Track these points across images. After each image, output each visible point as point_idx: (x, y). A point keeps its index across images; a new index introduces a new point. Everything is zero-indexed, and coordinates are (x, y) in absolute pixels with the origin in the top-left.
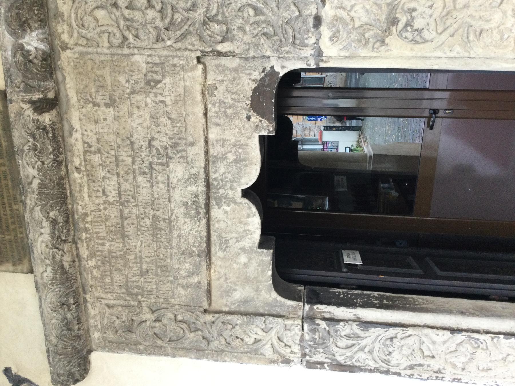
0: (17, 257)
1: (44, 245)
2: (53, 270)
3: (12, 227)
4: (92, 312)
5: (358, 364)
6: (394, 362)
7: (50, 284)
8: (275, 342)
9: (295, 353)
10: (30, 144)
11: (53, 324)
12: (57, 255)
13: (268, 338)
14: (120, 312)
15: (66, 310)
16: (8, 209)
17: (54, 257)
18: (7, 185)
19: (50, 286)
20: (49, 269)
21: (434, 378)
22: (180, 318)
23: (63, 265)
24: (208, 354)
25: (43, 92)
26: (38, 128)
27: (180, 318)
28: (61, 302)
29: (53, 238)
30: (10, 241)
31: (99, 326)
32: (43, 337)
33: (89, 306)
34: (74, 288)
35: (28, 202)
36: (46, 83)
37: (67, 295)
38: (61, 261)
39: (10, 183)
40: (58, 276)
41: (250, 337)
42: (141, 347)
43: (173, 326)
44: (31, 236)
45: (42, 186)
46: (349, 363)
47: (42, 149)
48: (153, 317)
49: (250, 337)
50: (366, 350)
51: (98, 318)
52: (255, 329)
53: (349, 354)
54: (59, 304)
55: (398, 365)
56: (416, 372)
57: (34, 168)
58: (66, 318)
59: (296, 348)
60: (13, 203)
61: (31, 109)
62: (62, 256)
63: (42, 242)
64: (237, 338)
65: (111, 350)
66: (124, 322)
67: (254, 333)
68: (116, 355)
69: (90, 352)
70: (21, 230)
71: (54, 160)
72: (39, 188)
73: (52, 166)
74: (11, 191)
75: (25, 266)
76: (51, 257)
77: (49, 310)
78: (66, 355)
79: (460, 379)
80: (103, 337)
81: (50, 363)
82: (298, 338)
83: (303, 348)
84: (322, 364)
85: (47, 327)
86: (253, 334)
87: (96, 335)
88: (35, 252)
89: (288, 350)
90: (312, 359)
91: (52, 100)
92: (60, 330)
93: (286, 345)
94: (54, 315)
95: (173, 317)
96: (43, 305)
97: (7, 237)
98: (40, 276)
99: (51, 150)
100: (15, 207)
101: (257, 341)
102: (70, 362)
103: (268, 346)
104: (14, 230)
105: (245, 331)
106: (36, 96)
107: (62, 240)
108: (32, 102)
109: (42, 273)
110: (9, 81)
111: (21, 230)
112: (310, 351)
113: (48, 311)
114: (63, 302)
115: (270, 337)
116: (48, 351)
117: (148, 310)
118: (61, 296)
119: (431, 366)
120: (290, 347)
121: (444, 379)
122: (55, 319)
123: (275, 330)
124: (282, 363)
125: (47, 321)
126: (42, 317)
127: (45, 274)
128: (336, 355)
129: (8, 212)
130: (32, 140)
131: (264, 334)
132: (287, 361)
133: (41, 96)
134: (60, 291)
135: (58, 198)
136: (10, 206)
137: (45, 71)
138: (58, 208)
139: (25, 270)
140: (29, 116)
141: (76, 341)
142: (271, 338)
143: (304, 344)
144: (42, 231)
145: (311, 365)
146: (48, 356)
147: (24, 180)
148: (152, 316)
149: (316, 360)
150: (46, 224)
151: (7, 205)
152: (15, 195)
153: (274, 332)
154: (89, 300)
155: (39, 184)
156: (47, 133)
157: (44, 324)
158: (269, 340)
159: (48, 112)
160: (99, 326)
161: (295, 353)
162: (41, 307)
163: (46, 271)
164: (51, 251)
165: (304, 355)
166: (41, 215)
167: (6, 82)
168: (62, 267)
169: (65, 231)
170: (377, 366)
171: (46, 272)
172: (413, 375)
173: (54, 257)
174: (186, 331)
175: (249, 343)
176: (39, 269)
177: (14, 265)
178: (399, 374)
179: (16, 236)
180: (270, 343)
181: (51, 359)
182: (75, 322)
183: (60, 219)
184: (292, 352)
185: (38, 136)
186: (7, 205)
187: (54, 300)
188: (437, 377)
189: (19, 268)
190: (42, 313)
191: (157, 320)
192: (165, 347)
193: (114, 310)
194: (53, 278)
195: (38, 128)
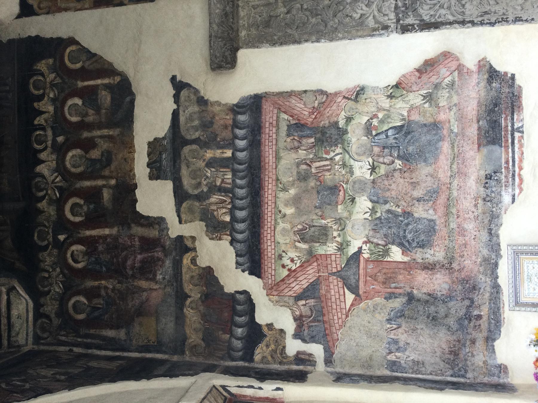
4: (242, 14)
5: (439, 20)
6: (467, 12)
8: (376, 13)
9: (391, 20)
13: (371, 11)
14: (262, 10)
21: (500, 20)
22: (305, 7)
24: (326, 33)
27: (305, 7)
31: (246, 25)
33: (240, 9)
41: (357, 13)
42: (276, 38)
43: (300, 14)
46: (433, 20)
48: (285, 10)
49: (357, 13)
50: (445, 6)
51: (246, 19)
52: (361, 5)
53: (432, 13)
55: (471, 15)
56: (486, 17)
59: (392, 16)
64: (347, 16)
65: (254, 46)
66: (264, 18)
67: (360, 8)
68: (256, 50)
69: (237, 49)
78: (223, 38)
79: (521, 17)
80: (248, 34)
82: (393, 6)
83: (397, 15)
84: (413, 25)
85: (212, 16)
86: (359, 9)
87: (243, 33)
89: (386, 18)
90: (405, 22)
93: (384, 15)
95: (300, 6)
101: (362, 15)
102: (225, 45)
103: (371, 17)
105: (353, 9)
112: (403, 16)
113: (214, 3)
115: (372, 10)
116: (210, 36)
117: (282, 5)
119: (497, 11)
120: (387, 15)
121: (508, 20)
123: (376, 3)
124: (382, 29)
125: (212, 11)
128: (423, 15)
131: (368, 9)
132: (386, 28)
142: (373, 11)
143: (398, 11)
145: (405, 29)
146: (210, 41)
148: (285, 9)
149: (407, 23)
153: (375, 5)
154: (240, 4)
157: (210, 14)
158: (371, 13)
160: (246, 25)
161: (391, 20)
165: (398, 21)
170: (455, 19)
172: (483, 20)
174: (310, 18)
175: (356, 18)
178: (473, 23)
180: (372, 15)
181: (212, 43)
184: (389, 19)
188: (502, 18)
191: (288, 13)
192: (293, 35)
193: (258, 10)
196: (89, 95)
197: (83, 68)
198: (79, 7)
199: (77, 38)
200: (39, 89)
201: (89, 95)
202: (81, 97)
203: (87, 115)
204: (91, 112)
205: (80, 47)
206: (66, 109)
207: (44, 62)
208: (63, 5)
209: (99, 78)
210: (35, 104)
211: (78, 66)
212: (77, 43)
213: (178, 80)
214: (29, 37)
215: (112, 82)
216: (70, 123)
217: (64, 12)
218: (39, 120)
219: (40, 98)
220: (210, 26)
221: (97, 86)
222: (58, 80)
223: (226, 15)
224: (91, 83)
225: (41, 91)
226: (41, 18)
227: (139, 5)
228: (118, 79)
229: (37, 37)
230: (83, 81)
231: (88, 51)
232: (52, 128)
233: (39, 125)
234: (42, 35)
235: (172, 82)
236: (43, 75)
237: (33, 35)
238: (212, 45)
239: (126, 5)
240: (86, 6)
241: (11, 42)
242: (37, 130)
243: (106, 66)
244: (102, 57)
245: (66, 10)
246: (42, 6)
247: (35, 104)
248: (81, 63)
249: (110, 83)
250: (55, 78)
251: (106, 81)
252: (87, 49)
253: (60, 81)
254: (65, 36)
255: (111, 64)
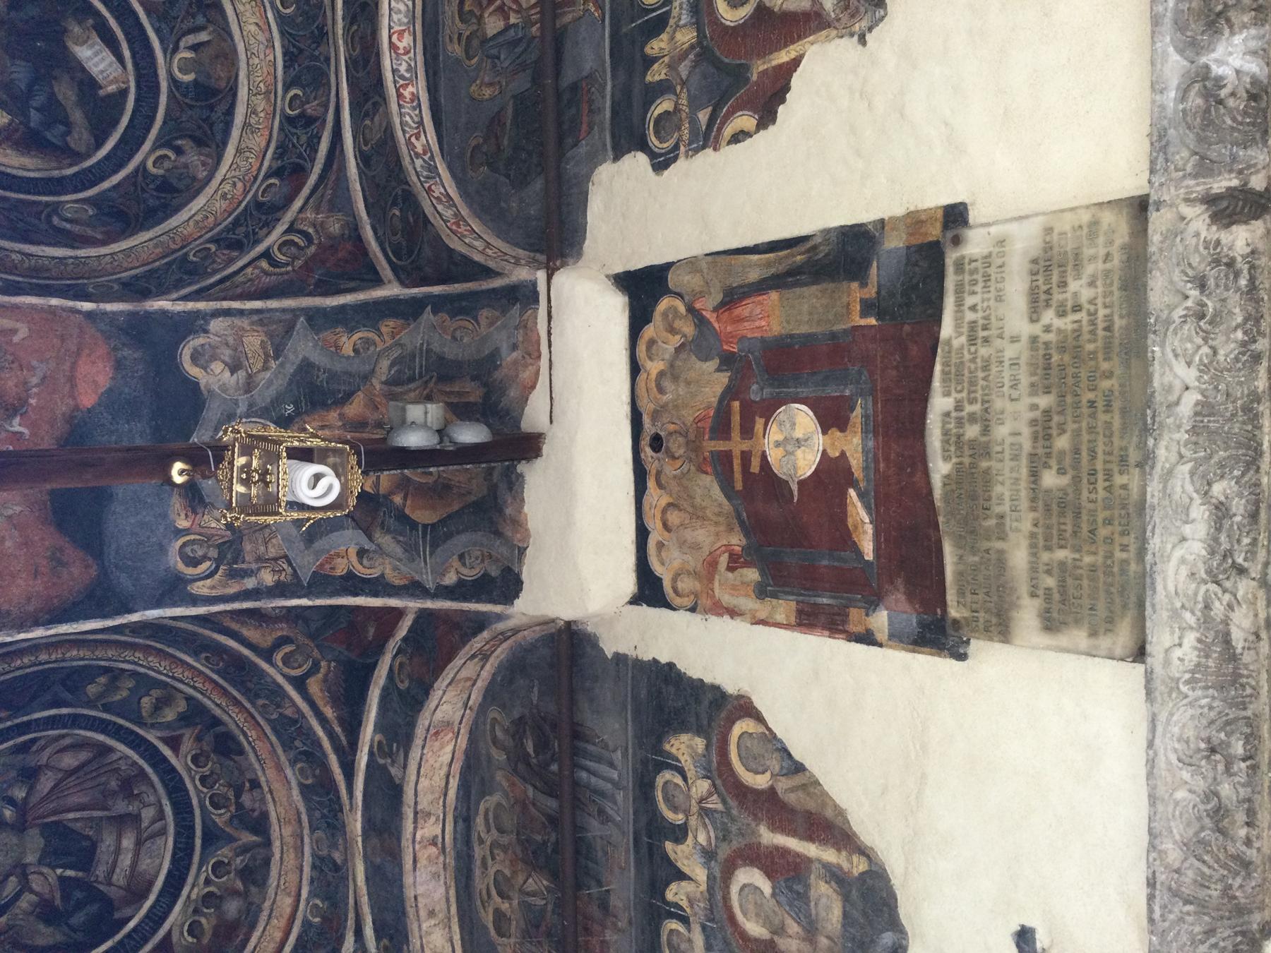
0: (1102, 611)
1: (1184, 571)
2: (1199, 641)
3: (1103, 532)
7: (1187, 682)
10: (1189, 303)
11: (1177, 803)
12: (1217, 604)
15: (1221, 767)
16: (1101, 484)
17: (1207, 607)
18: (1108, 425)
19: (1184, 689)
20: (1190, 639)
23: (1227, 634)
25: (1240, 172)
26: (1216, 262)
28: (1208, 740)
29: (1212, 553)
30: (1093, 568)
32: (1146, 838)
34: (1249, 713)
35: (1161, 453)
36: (1249, 152)
37: (1228, 723)
38: (1226, 622)
39: (1117, 423)
40: (1211, 663)
44: (1155, 543)
45: (1205, 409)
47: (1217, 314)
54: (1203, 746)
57: (1189, 364)
58: (1216, 794)
60: (1116, 469)
61: (1206, 216)
62: (1230, 607)
63: (1183, 561)
70: (1125, 540)
71: (1244, 344)
72: (1196, 414)
73: (1237, 359)
74: (1116, 440)
75: (1123, 638)
76: (1200, 606)
77: (1173, 758)
78: (1202, 906)
81: (1151, 920)
85: (1160, 808)
88: (1159, 587)
91: (1260, 195)
92: (1196, 826)
94: (1186, 775)
96: (1157, 741)
97: (1088, 559)
98: (1161, 656)
99: (1240, 319)
100: (1119, 480)
104: (1109, 540)
106: (1222, 183)
107: (1234, 565)
108: (1210, 200)
109: (1167, 651)
110: (1161, 159)
111: (1125, 540)
113: (1169, 763)
114: (1215, 742)
116: (1151, 883)
118: (1212, 722)
122: (1186, 789)
125: (1161, 791)
126: (1150, 775)
127: (1178, 653)
129: (1101, 494)
130: (1194, 293)
133: (1235, 183)
134: (1211, 708)
135: (1239, 445)
136: (1109, 476)
137: (1253, 124)
138: (1236, 473)
139: (1118, 651)
140: (1197, 235)
141: (1237, 874)
144: (1187, 530)
146: (1151, 898)
147: (1158, 398)
150: (1200, 512)
151: (1100, 476)
152: (1126, 449)
155: (1197, 404)
156: (1237, 275)
157: (1153, 799)
159: (1246, 223)
162: (1150, 744)
163: (1180, 645)
164: (1203, 588)
166: (1190, 488)
167: (1153, 162)
168: (1227, 640)
169: (1246, 541)
171: (1177, 646)
173: (1207, 607)
176: (1160, 639)
177: (1093, 634)
179: (1109, 555)
182: (1241, 817)
183: (1239, 507)
185: (1211, 282)
186: (1100, 476)
187: (1190, 733)
189: (1105, 642)
190: (1151, 763)
194: (1198, 665)
195: (1216, 262)
196: (789, 872)
197: (772, 791)
198: (762, 615)
199: (759, 703)
200: (675, 809)
201: (789, 872)
202: (769, 874)
203: (780, 930)
204: (793, 928)
205: (761, 729)
206: (734, 890)
207: (685, 737)
208: (727, 599)
209: (810, 839)
210: (669, 846)
211: (760, 781)
212: (759, 718)
213: (1039, 946)
214: (655, 661)
215: (845, 865)
216: (743, 935)
217: (726, 618)
218: (676, 893)
219: (679, 834)
220: (1152, 847)
221: (809, 860)
222: (715, 804)
223: (1219, 814)
224: (792, 843)
225: (679, 819)
226: (680, 619)
227: (920, 657)
228: (859, 866)
229: (671, 666)
230: (774, 828)
231: (785, 752)
232: (704, 928)
233: (677, 905)
234: (681, 666)
235: (1018, 946)
236: (681, 772)
237: (664, 659)
238: (1157, 915)
239: (881, 645)
240: (780, 617)
241: (620, 658)
242: (672, 916)
243: (829, 813)
244: (817, 783)
245: (733, 613)
246: (680, 585)
247: (669, 846)
248: (768, 774)
249: (840, 867)
250: (710, 794)
251: (829, 855)
252: (780, 741)
253: (720, 807)
254: (730, 689)
255: (841, 812)
